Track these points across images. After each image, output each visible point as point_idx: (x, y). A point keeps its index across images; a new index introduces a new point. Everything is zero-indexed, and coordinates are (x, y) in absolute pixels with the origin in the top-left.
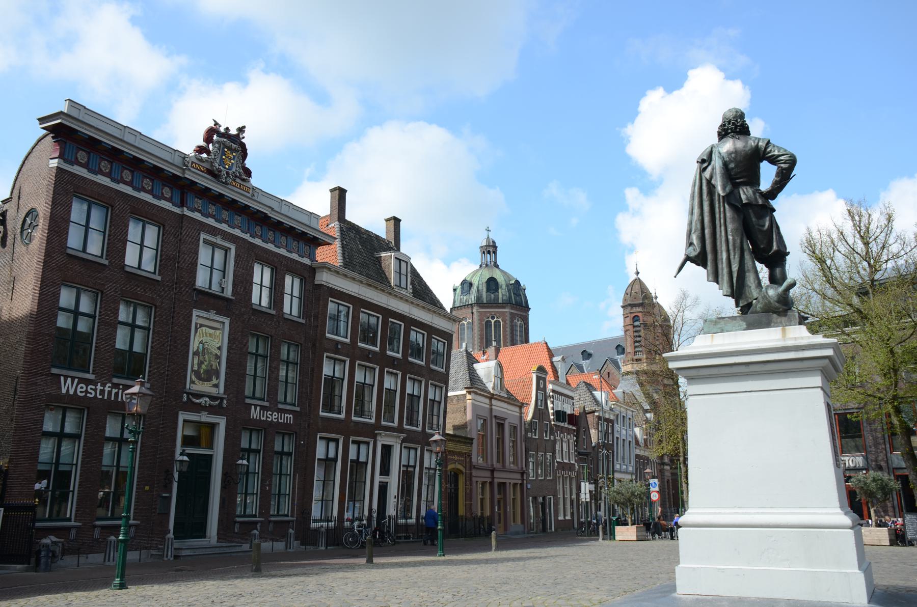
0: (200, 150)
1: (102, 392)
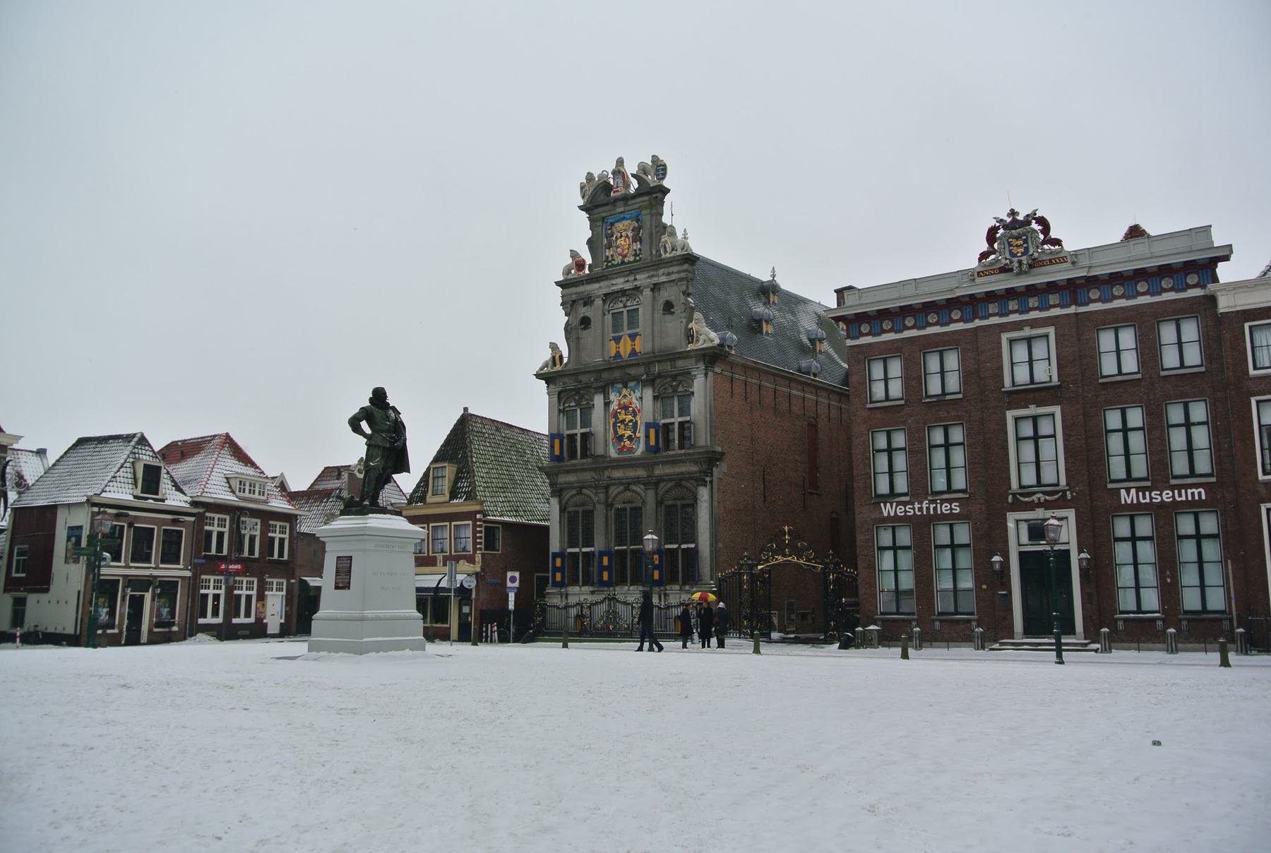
0: (984, 256)
1: (920, 509)
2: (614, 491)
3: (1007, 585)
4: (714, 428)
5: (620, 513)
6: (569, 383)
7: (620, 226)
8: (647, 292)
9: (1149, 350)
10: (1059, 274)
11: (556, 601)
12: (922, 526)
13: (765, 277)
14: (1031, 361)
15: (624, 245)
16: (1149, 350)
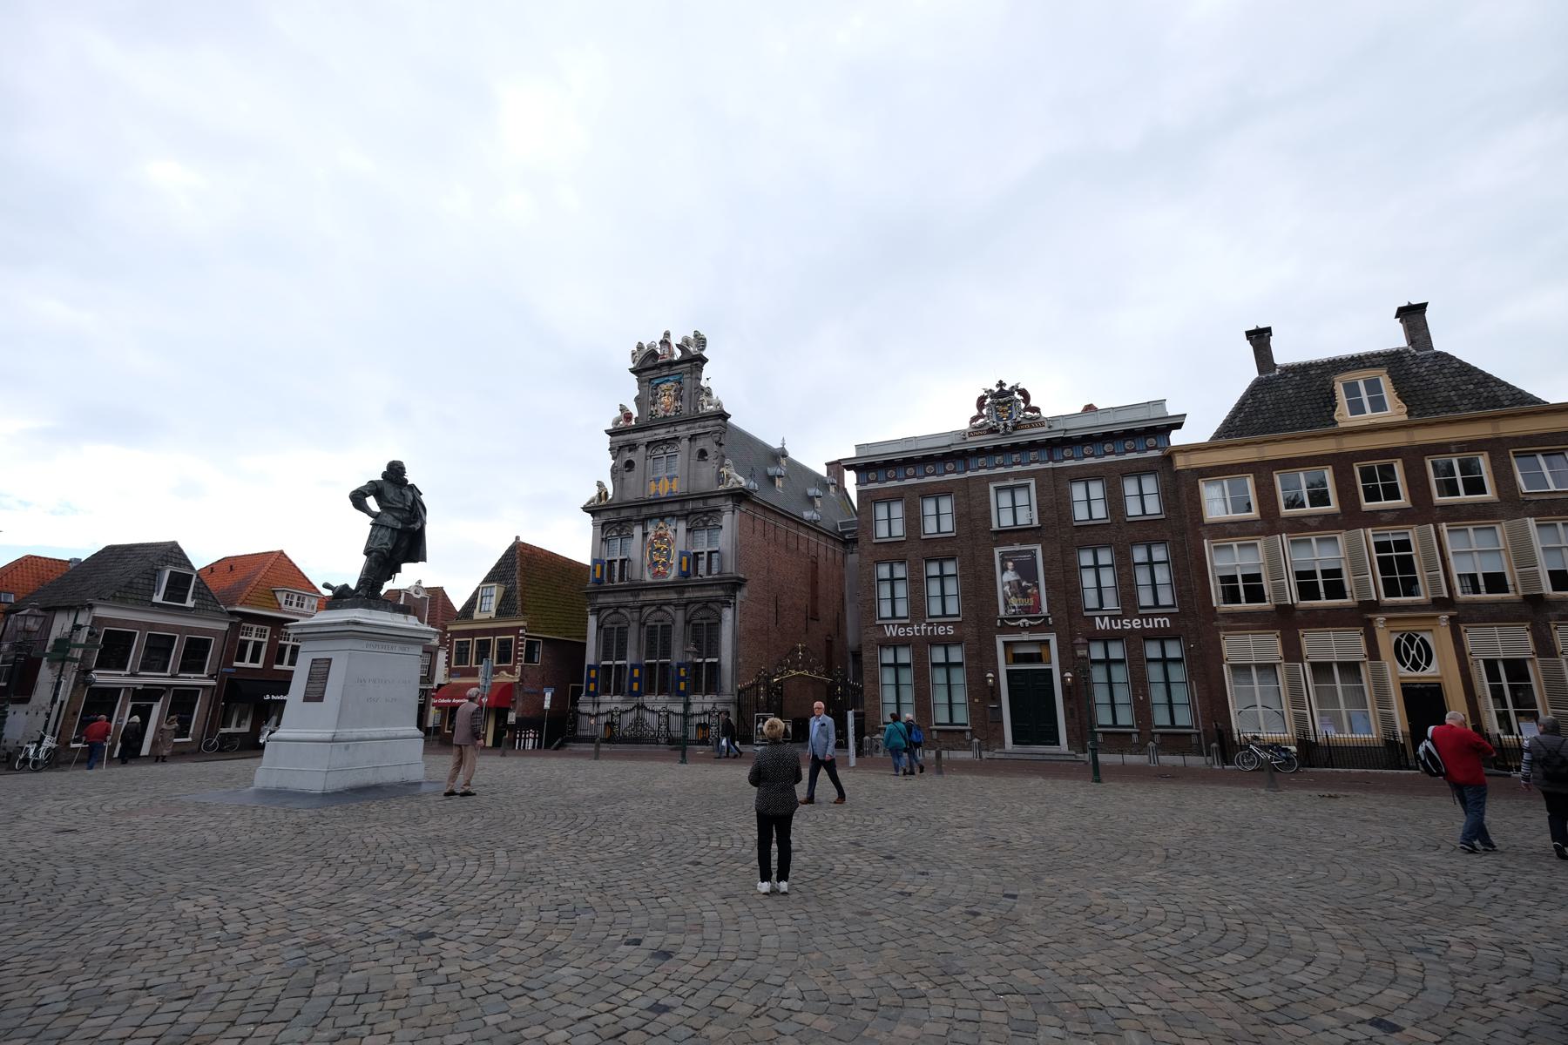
0: (974, 419)
2: (647, 611)
3: (996, 697)
4: (739, 559)
5: (652, 631)
6: (609, 515)
7: (664, 386)
8: (685, 442)
9: (1115, 501)
10: (1038, 434)
11: (588, 709)
12: (921, 646)
13: (776, 445)
14: (1014, 508)
15: (666, 403)
16: (1115, 501)
